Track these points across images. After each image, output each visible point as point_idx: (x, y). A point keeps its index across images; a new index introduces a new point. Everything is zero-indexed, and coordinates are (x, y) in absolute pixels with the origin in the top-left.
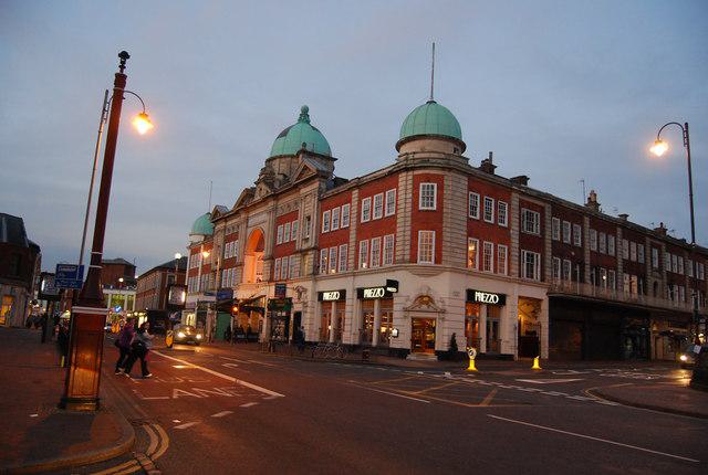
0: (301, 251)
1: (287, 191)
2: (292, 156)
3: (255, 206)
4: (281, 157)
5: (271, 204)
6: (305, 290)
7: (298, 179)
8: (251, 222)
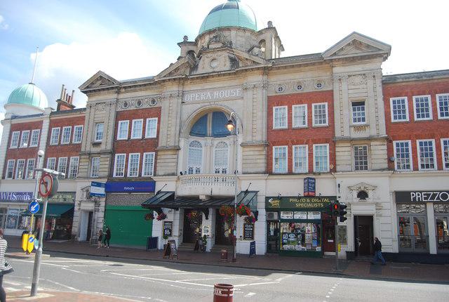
0: (351, 140)
1: (307, 65)
2: (252, 32)
3: (205, 77)
4: (239, 29)
5: (256, 78)
6: (374, 188)
7: (335, 54)
8: (188, 98)
